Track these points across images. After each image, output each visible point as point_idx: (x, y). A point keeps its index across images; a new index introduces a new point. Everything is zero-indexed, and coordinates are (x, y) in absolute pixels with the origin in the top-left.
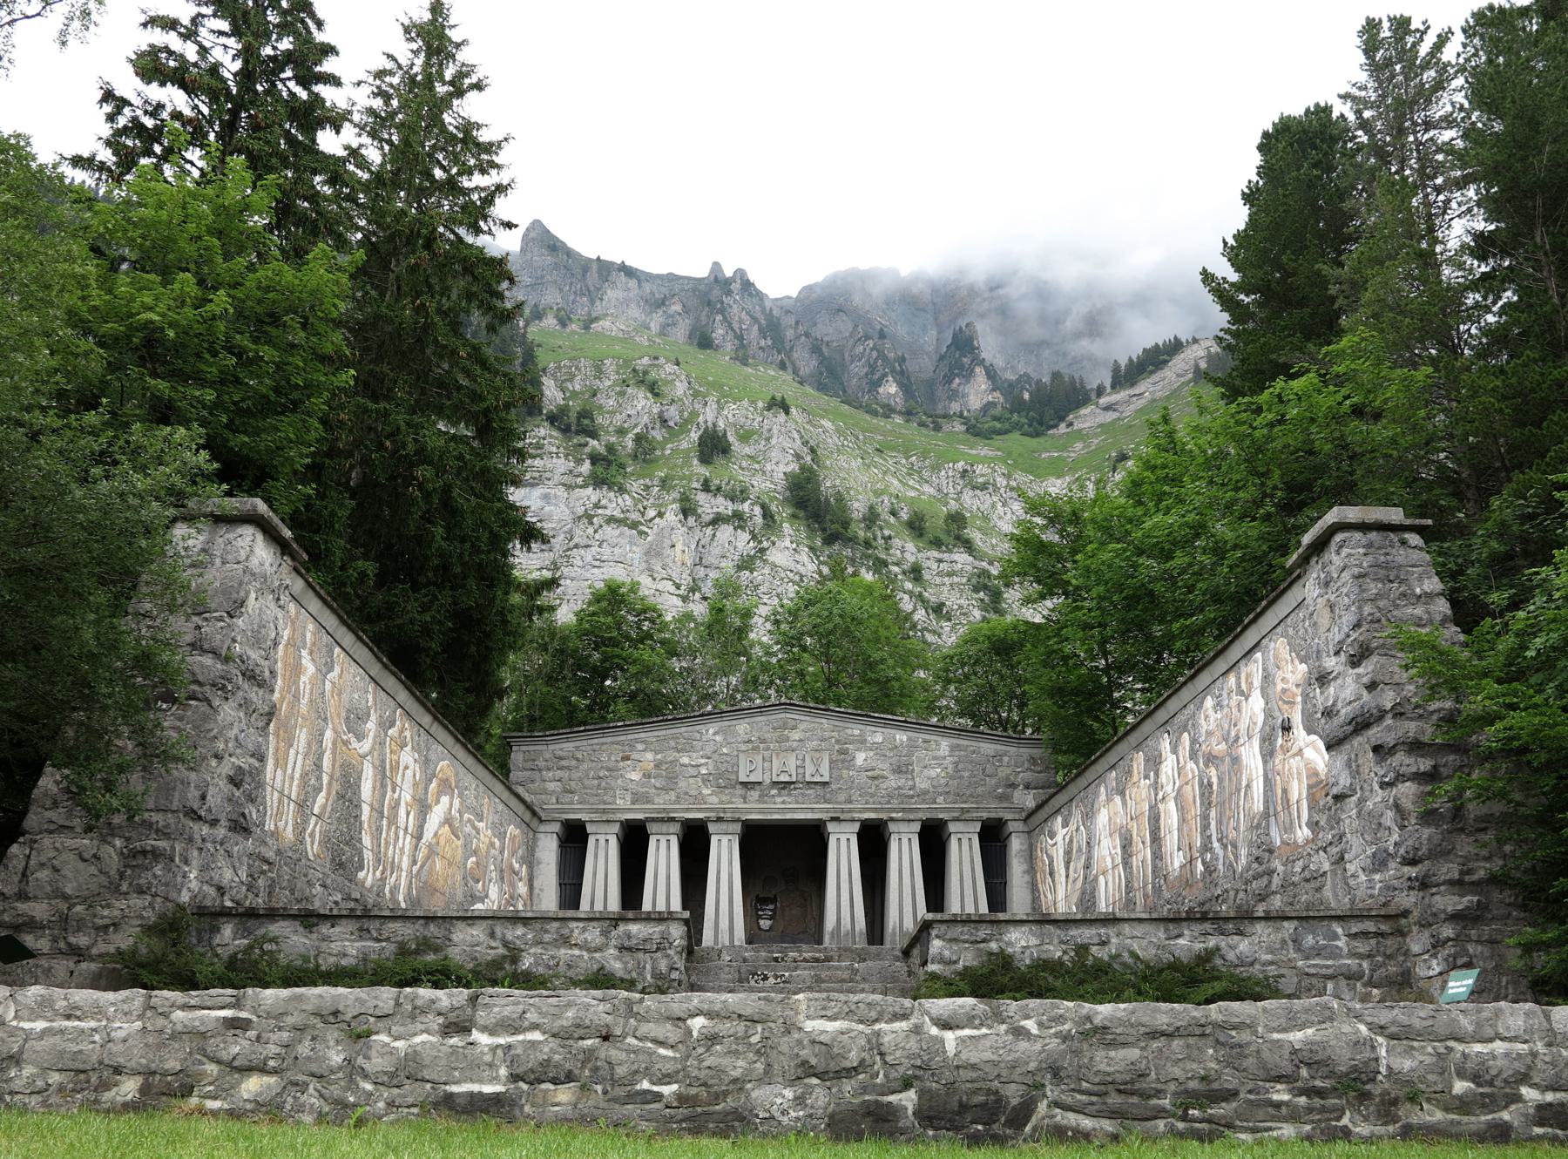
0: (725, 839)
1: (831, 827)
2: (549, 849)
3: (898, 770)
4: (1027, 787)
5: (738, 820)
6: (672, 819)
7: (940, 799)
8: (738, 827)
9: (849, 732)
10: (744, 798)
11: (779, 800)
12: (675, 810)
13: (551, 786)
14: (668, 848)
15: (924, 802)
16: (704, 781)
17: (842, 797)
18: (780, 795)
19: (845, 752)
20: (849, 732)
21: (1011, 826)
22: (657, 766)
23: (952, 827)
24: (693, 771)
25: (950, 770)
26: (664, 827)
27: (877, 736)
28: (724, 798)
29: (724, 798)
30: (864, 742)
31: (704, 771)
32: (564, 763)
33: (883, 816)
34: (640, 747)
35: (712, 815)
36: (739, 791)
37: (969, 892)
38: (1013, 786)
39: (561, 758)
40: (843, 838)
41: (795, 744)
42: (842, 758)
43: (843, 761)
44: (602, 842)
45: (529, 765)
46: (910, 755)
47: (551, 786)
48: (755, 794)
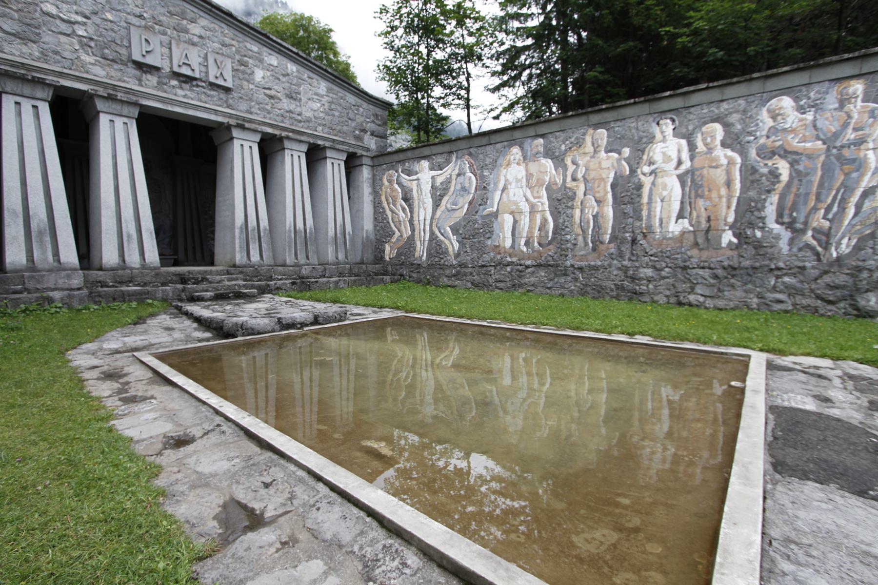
1: (235, 133)
3: (290, 97)
4: (372, 134)
5: (135, 104)
7: (320, 128)
9: (248, 45)
10: (140, 80)
11: (180, 92)
14: (37, 116)
15: (308, 128)
17: (243, 106)
18: (181, 88)
19: (245, 64)
20: (248, 45)
21: (365, 161)
23: (329, 153)
25: (326, 107)
27: (273, 60)
30: (261, 61)
33: (284, 134)
36: (132, 71)
37: (338, 203)
38: (364, 131)
40: (247, 145)
41: (196, 39)
42: (242, 69)
43: (244, 72)
46: (299, 85)
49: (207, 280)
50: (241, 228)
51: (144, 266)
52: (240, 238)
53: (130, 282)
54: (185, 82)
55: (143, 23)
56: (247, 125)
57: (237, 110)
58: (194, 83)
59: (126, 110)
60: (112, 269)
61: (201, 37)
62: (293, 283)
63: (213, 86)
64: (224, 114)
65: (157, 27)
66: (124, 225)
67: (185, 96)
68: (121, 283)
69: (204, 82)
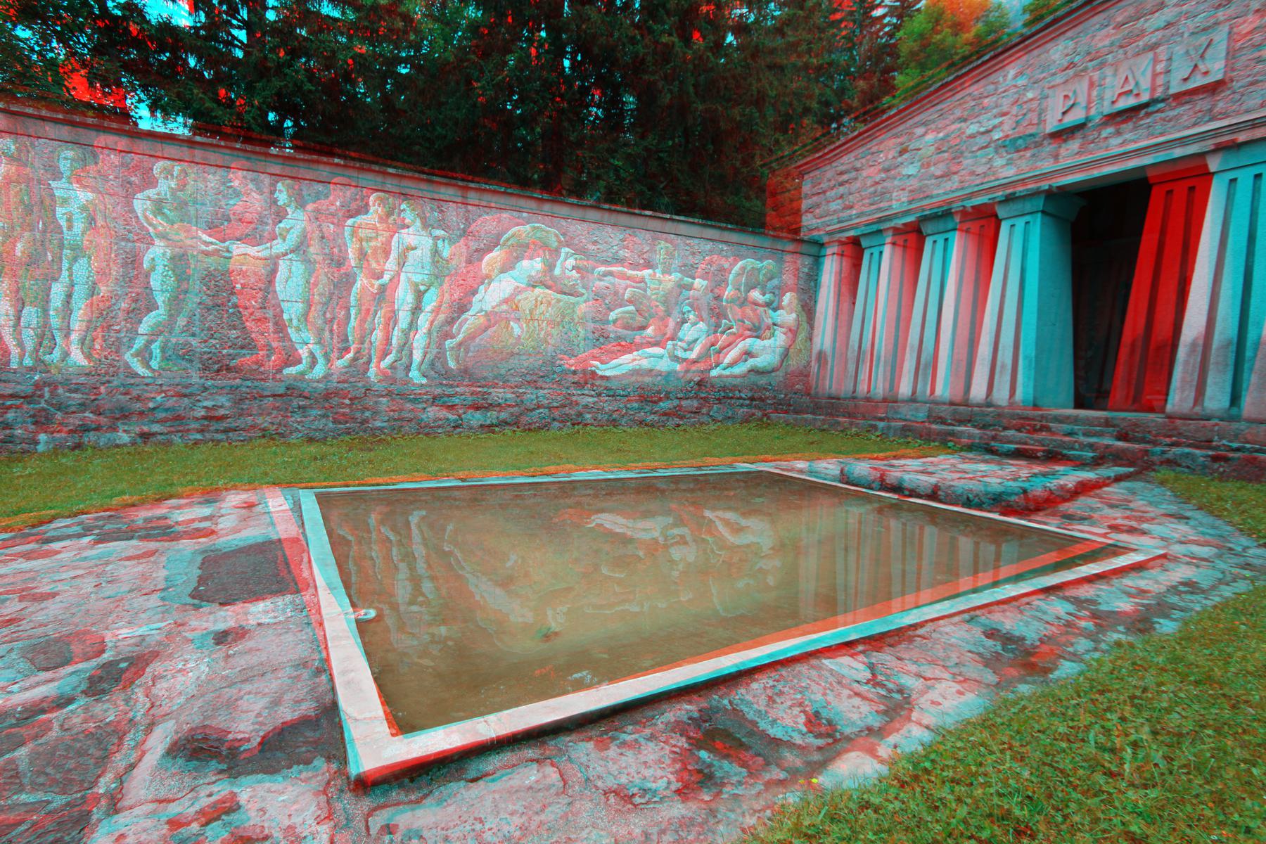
0: (1020, 223)
2: (831, 268)
5: (1036, 193)
6: (947, 214)
8: (1039, 203)
12: (955, 200)
13: (833, 206)
16: (996, 151)
18: (1118, 133)
22: (939, 150)
24: (982, 141)
26: (941, 225)
28: (1023, 164)
29: (1024, 166)
31: (997, 135)
32: (845, 177)
34: (919, 131)
35: (999, 194)
36: (1049, 147)
39: (841, 173)
41: (1154, 39)
44: (876, 255)
45: (815, 190)
47: (833, 206)
48: (1074, 145)
49: (1048, 429)
50: (1194, 345)
51: (989, 404)
52: (1186, 363)
53: (969, 421)
54: (1124, 122)
55: (1071, 72)
56: (1242, 137)
57: (1238, 113)
58: (1143, 113)
59: (1028, 206)
60: (979, 406)
61: (1169, 25)
62: (1215, 459)
63: (1177, 96)
64: (1182, 141)
65: (1090, 64)
66: (1000, 353)
67: (1122, 144)
68: (961, 422)
69: (1163, 100)
